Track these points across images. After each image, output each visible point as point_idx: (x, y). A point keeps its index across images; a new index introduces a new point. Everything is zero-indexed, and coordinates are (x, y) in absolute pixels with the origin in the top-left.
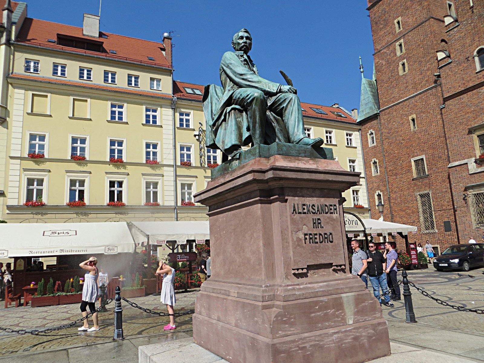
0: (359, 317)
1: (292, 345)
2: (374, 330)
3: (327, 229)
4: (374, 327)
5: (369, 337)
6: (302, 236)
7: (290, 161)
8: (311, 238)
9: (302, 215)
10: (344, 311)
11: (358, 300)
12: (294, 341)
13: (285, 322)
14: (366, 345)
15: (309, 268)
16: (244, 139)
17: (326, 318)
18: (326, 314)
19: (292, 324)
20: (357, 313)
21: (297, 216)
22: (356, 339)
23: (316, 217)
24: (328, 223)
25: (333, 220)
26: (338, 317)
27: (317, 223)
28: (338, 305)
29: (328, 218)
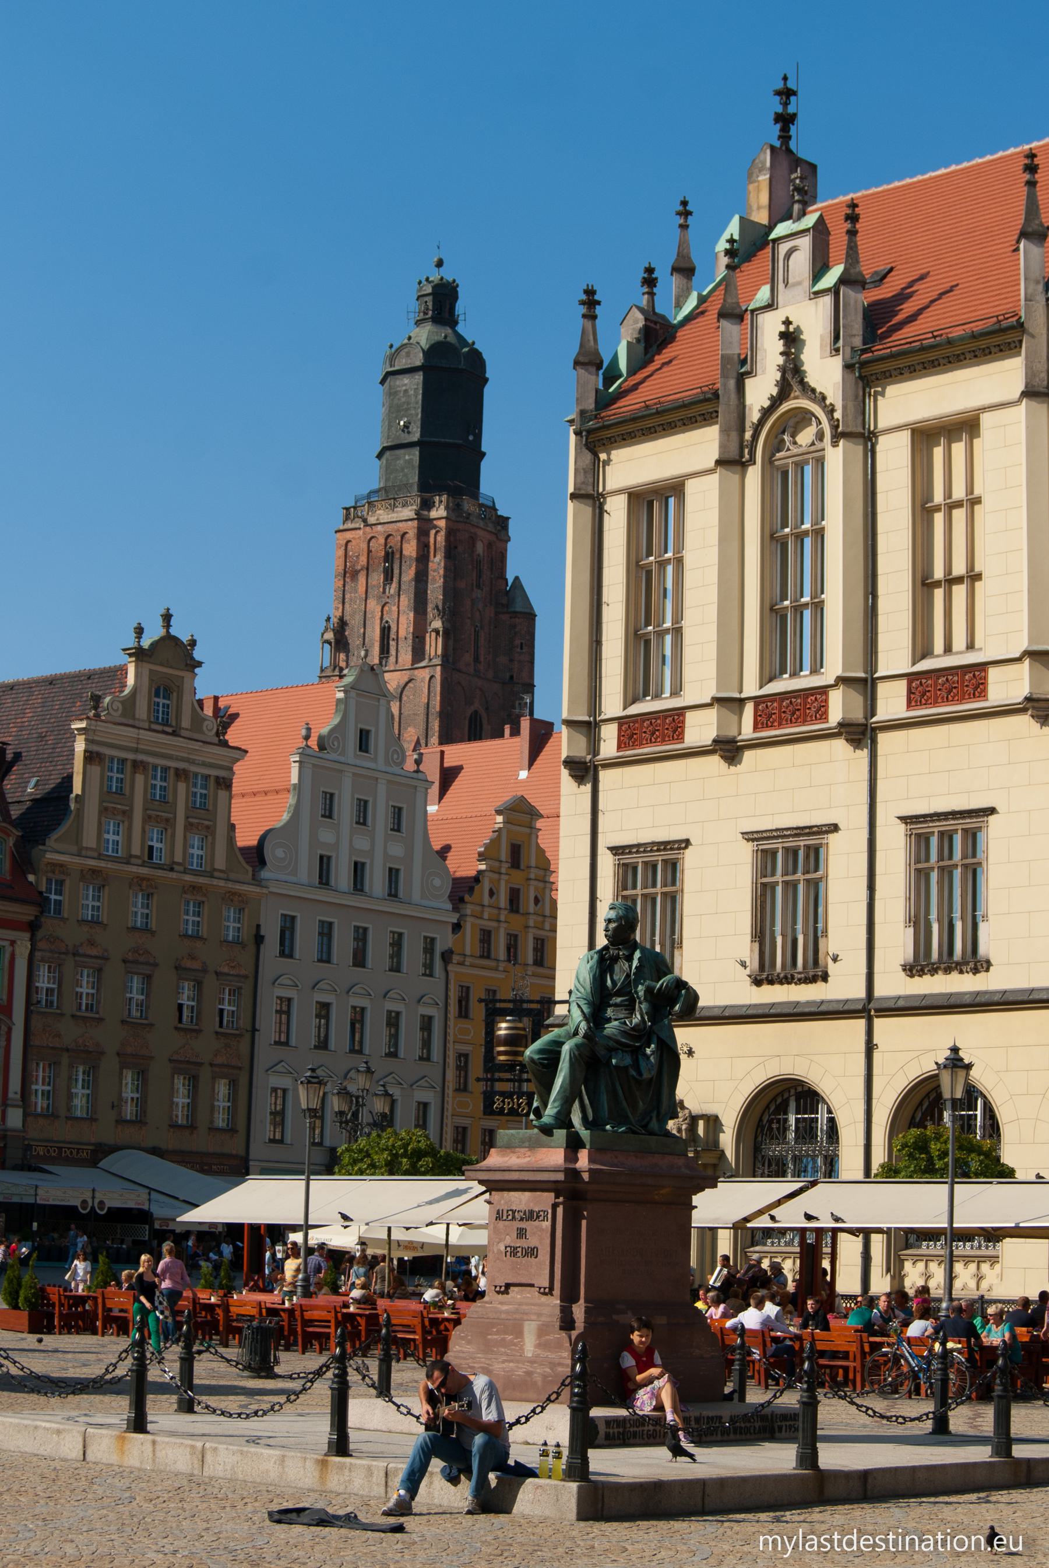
0: (539, 1352)
1: (462, 1361)
2: (551, 1369)
3: (532, 1241)
4: (553, 1365)
5: (545, 1377)
6: (503, 1248)
7: (503, 1156)
8: (513, 1251)
9: (507, 1223)
10: (523, 1340)
11: (542, 1332)
12: (465, 1359)
13: (462, 1338)
14: (540, 1384)
15: (508, 1286)
16: (577, 1103)
17: (503, 1343)
18: (503, 1340)
19: (469, 1342)
20: (538, 1346)
21: (501, 1224)
22: (529, 1373)
23: (523, 1225)
24: (534, 1233)
25: (542, 1230)
26: (515, 1345)
27: (521, 1233)
28: (519, 1333)
29: (536, 1227)
